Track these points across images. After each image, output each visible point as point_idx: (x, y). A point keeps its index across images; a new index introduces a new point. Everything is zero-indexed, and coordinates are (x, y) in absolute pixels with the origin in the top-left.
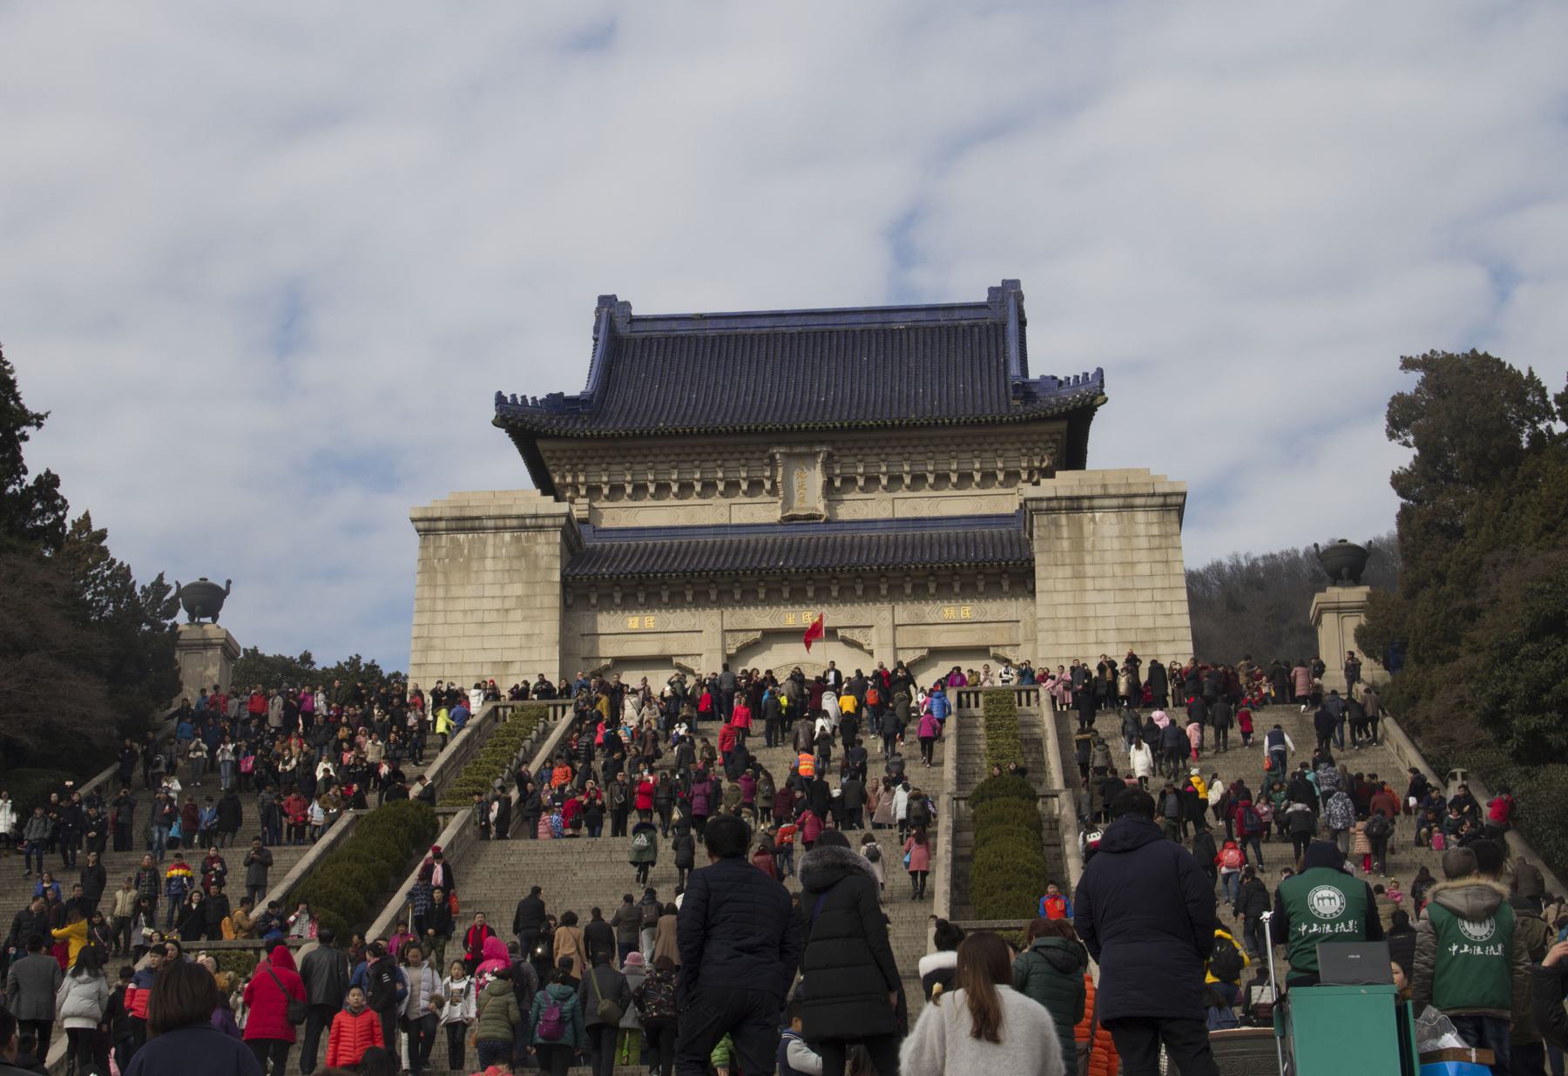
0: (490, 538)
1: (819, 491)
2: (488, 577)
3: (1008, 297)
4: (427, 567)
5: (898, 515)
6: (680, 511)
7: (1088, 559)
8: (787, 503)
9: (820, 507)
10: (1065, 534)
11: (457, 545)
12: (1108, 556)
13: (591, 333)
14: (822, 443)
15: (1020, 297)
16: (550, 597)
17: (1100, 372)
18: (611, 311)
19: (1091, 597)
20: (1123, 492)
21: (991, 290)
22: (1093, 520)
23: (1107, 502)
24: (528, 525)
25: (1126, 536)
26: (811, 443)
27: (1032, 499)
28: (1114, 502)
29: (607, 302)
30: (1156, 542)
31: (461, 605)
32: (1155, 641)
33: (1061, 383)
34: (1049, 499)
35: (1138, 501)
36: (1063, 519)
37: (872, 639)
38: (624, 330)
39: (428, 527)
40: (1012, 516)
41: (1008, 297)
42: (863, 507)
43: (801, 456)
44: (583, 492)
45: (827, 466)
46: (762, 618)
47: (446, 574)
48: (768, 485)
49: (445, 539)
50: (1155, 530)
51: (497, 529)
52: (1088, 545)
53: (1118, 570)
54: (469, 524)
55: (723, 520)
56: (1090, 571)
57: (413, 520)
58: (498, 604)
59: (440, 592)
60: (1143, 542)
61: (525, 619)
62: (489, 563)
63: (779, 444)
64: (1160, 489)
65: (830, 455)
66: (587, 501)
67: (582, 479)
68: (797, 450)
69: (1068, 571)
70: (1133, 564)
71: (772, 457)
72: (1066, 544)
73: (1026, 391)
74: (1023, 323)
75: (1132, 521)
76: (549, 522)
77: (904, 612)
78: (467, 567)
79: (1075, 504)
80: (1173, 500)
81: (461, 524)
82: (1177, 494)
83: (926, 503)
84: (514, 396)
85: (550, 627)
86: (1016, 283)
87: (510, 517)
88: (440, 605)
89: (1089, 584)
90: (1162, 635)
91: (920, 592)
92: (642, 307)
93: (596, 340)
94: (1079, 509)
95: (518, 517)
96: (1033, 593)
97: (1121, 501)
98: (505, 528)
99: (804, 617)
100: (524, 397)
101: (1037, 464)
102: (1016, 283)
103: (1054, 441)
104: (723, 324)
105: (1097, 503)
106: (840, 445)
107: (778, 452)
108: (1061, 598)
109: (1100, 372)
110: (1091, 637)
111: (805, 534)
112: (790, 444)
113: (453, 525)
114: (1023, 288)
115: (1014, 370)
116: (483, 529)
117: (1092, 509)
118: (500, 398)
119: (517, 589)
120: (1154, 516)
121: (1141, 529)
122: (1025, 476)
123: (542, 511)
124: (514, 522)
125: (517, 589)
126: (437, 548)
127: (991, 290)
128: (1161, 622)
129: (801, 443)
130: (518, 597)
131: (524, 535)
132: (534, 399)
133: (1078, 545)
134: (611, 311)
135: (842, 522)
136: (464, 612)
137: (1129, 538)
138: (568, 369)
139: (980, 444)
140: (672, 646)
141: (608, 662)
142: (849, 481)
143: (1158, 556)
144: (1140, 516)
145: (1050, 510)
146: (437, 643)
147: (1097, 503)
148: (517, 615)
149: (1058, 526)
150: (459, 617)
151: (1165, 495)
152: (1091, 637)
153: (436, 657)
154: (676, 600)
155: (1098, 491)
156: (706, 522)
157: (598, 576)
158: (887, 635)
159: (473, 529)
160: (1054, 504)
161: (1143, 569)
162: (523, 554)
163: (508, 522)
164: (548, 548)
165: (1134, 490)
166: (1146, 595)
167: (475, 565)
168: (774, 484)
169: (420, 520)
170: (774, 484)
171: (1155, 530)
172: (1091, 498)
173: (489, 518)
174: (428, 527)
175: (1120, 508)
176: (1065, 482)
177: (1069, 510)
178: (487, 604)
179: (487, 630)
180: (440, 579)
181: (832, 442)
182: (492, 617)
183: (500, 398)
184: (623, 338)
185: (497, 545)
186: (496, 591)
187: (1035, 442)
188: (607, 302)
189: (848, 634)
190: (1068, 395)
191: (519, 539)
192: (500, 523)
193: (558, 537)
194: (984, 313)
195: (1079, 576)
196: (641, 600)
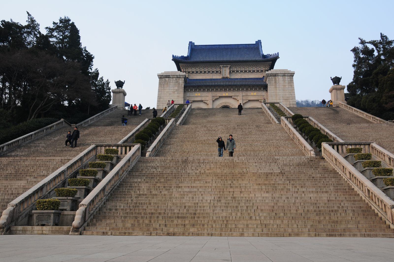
1: (228, 73)
2: (171, 86)
3: (259, 43)
4: (160, 84)
6: (204, 76)
7: (277, 85)
9: (228, 76)
10: (273, 80)
11: (166, 80)
12: (281, 84)
13: (188, 48)
14: (229, 65)
15: (261, 43)
16: (182, 90)
17: (278, 53)
18: (191, 44)
19: (278, 91)
20: (284, 73)
21: (256, 42)
22: (278, 78)
23: (281, 75)
24: (178, 77)
25: (284, 81)
26: (227, 65)
27: (267, 74)
28: (282, 75)
29: (191, 43)
30: (289, 82)
31: (167, 91)
32: (289, 99)
33: (271, 55)
34: (270, 74)
35: (286, 75)
36: (273, 78)
37: (238, 98)
38: (193, 47)
39: (161, 77)
40: (262, 78)
41: (259, 43)
43: (225, 67)
44: (187, 73)
45: (230, 68)
46: (219, 94)
47: (164, 86)
48: (219, 72)
49: (163, 79)
50: (289, 80)
51: (173, 78)
52: (277, 82)
53: (283, 87)
54: (168, 77)
55: (211, 78)
56: (278, 86)
57: (158, 76)
58: (173, 91)
60: (287, 82)
61: (177, 93)
63: (221, 65)
64: (290, 73)
65: (230, 67)
67: (187, 70)
68: (224, 66)
69: (274, 87)
70: (285, 86)
71: (220, 67)
72: (273, 82)
73: (264, 56)
75: (285, 78)
76: (182, 76)
77: (244, 93)
79: (275, 75)
80: (292, 74)
81: (166, 77)
82: (293, 73)
83: (247, 76)
84: (175, 56)
85: (182, 95)
86: (260, 41)
87: (175, 75)
89: (278, 89)
90: (291, 98)
91: (247, 90)
92: (197, 43)
93: (189, 49)
94: (276, 76)
95: (176, 75)
96: (267, 91)
97: (283, 75)
99: (227, 94)
100: (177, 56)
101: (266, 69)
102: (260, 41)
103: (269, 65)
104: (210, 46)
105: (279, 75)
106: (232, 65)
107: (221, 66)
108: (272, 91)
109: (278, 53)
110: (278, 98)
112: (223, 65)
113: (165, 77)
116: (170, 77)
118: (173, 56)
119: (176, 88)
120: (289, 77)
121: (287, 79)
123: (181, 74)
124: (176, 76)
125: (176, 88)
126: (162, 81)
127: (256, 42)
128: (290, 96)
129: (225, 65)
130: (176, 89)
131: (177, 79)
132: (179, 56)
133: (276, 82)
134: (191, 44)
135: (232, 79)
136: (167, 92)
137: (284, 81)
138: (184, 52)
139: (256, 65)
140: (203, 99)
141: (192, 101)
142: (233, 71)
143: (290, 84)
144: (286, 77)
145: (270, 76)
146: (162, 97)
147: (279, 75)
148: (176, 93)
149: (272, 79)
150: (166, 93)
151: (291, 74)
152: (278, 98)
154: (204, 90)
155: (279, 73)
156: (208, 78)
157: (190, 86)
158: (241, 98)
159: (168, 78)
160: (271, 75)
161: (287, 86)
162: (177, 82)
163: (175, 76)
164: (181, 81)
165: (286, 73)
166: (288, 91)
167: (169, 84)
168: (220, 72)
169: (159, 76)
170: (220, 72)
171: (289, 80)
172: (278, 74)
173: (171, 75)
174: (161, 77)
175: (283, 76)
177: (274, 76)
178: (171, 91)
179: (171, 95)
180: (163, 86)
181: (231, 65)
182: (172, 93)
183: (173, 56)
186: (172, 88)
187: (266, 65)
188: (191, 43)
189: (234, 97)
191: (176, 79)
192: (173, 76)
193: (183, 79)
194: (255, 45)
195: (276, 87)
196: (198, 90)
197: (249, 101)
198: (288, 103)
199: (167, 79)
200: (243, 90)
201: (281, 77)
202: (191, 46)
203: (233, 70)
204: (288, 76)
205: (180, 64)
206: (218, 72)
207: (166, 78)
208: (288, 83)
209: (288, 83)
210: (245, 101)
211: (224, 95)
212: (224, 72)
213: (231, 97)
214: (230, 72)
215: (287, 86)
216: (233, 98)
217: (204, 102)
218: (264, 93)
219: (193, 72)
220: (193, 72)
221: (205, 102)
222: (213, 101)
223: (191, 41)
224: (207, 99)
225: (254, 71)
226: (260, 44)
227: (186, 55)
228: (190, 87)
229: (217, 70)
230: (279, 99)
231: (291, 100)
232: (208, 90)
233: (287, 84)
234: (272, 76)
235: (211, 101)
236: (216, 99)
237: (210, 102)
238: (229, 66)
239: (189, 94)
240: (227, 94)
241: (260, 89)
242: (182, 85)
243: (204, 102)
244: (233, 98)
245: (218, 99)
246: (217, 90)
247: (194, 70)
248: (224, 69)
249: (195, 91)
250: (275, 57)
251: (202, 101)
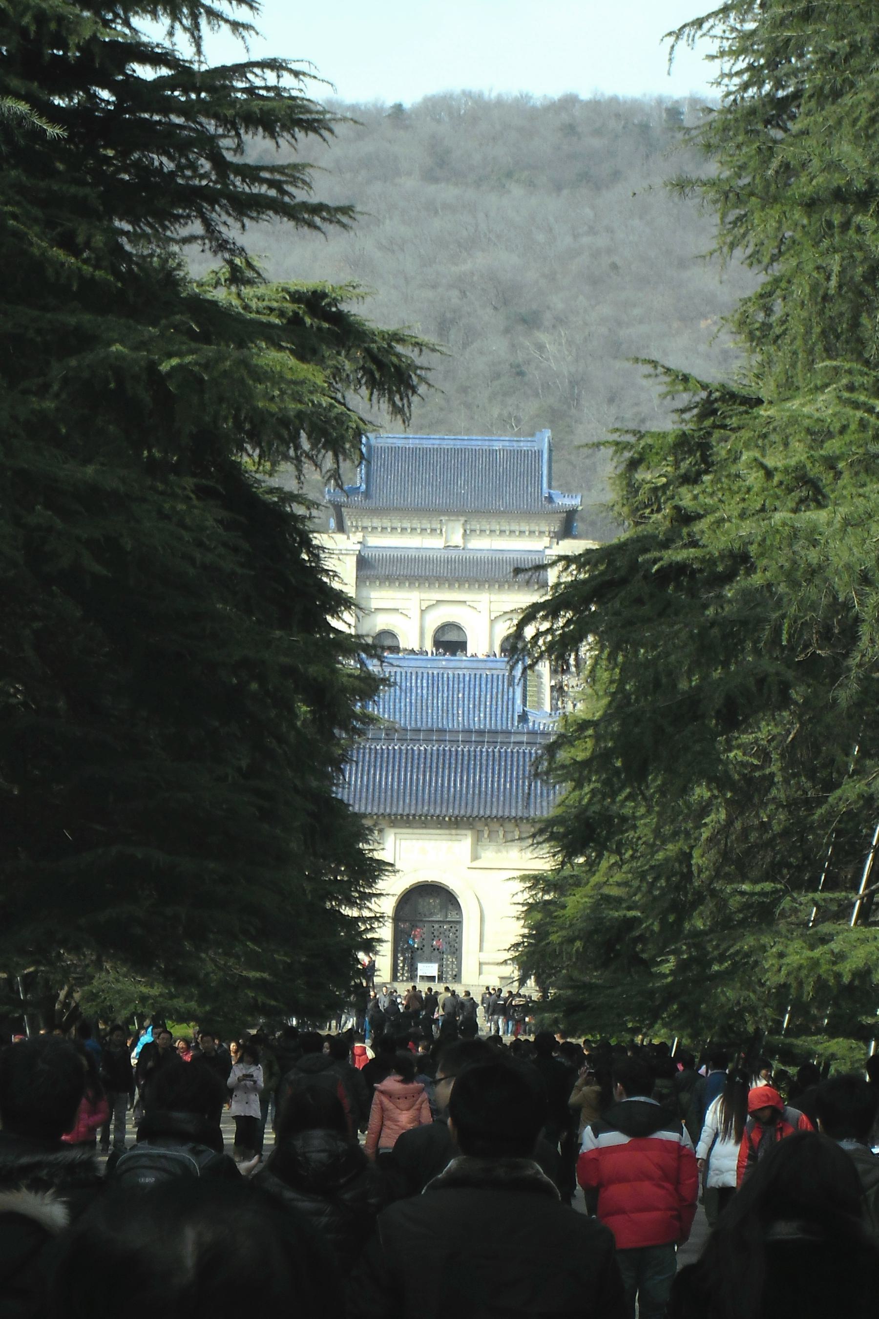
5: (493, 548)
8: (446, 541)
26: (458, 516)
48: (439, 531)
55: (419, 546)
63: (444, 515)
66: (361, 534)
76: (352, 552)
77: (495, 597)
111: (453, 554)
112: (448, 516)
122: (547, 533)
189: (471, 604)
203: (473, 527)
219: (374, 528)
221: (403, 611)
229: (434, 526)
237: (415, 614)
238: (462, 519)
245: (433, 605)
247: (376, 522)
248: (451, 524)
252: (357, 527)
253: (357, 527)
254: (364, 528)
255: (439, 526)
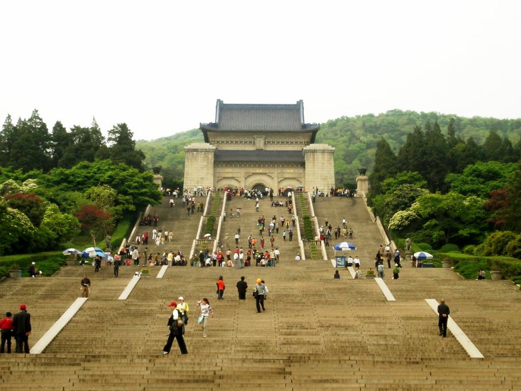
0: (200, 153)
2: (199, 161)
9: (263, 148)
10: (311, 157)
11: (193, 154)
15: (303, 103)
16: (211, 166)
24: (207, 151)
25: (323, 158)
26: (261, 135)
37: (273, 175)
42: (271, 148)
43: (260, 137)
46: (252, 170)
50: (329, 157)
51: (201, 152)
55: (243, 149)
56: (316, 164)
58: (201, 166)
59: (190, 164)
60: (326, 159)
62: (199, 158)
65: (265, 138)
73: (304, 126)
74: (303, 109)
78: (195, 158)
79: (314, 152)
85: (211, 171)
88: (190, 166)
89: (316, 167)
91: (283, 166)
93: (216, 108)
94: (314, 152)
96: (304, 168)
98: (202, 151)
99: (261, 171)
102: (302, 100)
107: (255, 136)
108: (310, 169)
112: (258, 135)
114: (304, 102)
115: (302, 122)
117: (317, 152)
118: (201, 124)
119: (205, 163)
120: (328, 154)
121: (326, 156)
125: (205, 163)
129: (260, 135)
133: (314, 160)
138: (210, 117)
140: (235, 176)
142: (269, 142)
144: (326, 154)
145: (308, 152)
148: (205, 169)
153: (189, 176)
154: (236, 166)
158: (276, 174)
159: (197, 151)
161: (326, 164)
164: (211, 156)
172: (317, 150)
175: (322, 152)
176: (312, 146)
177: (312, 152)
180: (190, 161)
181: (266, 135)
183: (201, 124)
184: (223, 108)
185: (201, 156)
188: (219, 100)
190: (312, 128)
193: (213, 153)
195: (314, 165)
197: (285, 178)
198: (327, 183)
199: (195, 153)
200: (278, 166)
201: (320, 154)
202: (220, 104)
203: (269, 141)
204: (327, 152)
205: (208, 133)
206: (251, 142)
207: (195, 151)
208: (328, 161)
209: (328, 161)
210: (281, 179)
211: (258, 171)
212: (258, 143)
213: (266, 174)
214: (265, 142)
215: (326, 164)
216: (268, 175)
217: (236, 180)
218: (301, 171)
219: (223, 142)
220: (223, 142)
222: (246, 178)
223: (219, 99)
224: (239, 175)
225: (292, 143)
226: (301, 104)
227: (214, 122)
228: (220, 162)
229: (251, 140)
230: (317, 178)
231: (329, 180)
232: (241, 166)
233: (326, 162)
234: (310, 152)
235: (243, 179)
236: (249, 176)
237: (242, 179)
238: (264, 136)
239: (219, 170)
240: (261, 171)
241: (297, 166)
242: (211, 160)
243: (236, 180)
244: (268, 175)
246: (250, 166)
247: (223, 139)
249: (226, 166)
250: (315, 129)
251: (233, 178)
252: (214, 141)
253: (214, 141)
254: (218, 142)
255: (253, 140)
